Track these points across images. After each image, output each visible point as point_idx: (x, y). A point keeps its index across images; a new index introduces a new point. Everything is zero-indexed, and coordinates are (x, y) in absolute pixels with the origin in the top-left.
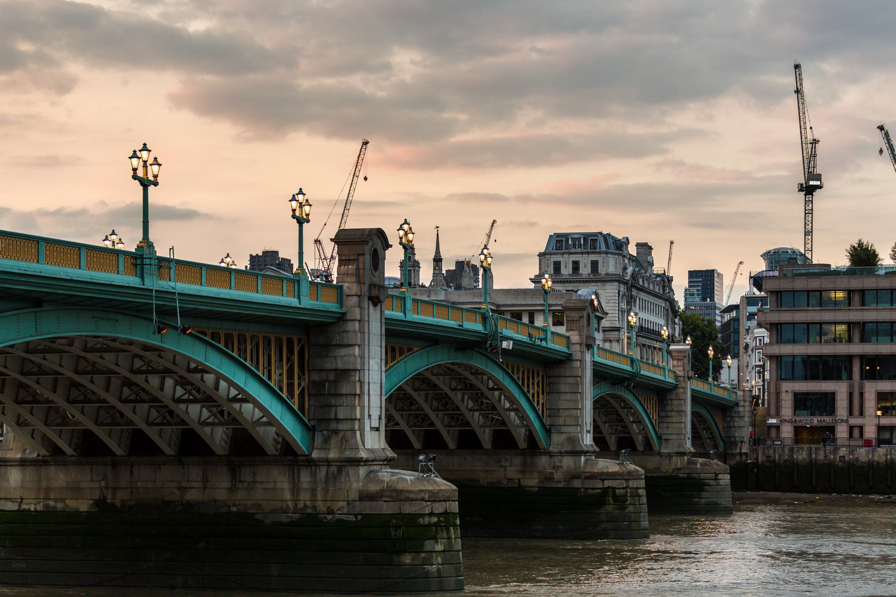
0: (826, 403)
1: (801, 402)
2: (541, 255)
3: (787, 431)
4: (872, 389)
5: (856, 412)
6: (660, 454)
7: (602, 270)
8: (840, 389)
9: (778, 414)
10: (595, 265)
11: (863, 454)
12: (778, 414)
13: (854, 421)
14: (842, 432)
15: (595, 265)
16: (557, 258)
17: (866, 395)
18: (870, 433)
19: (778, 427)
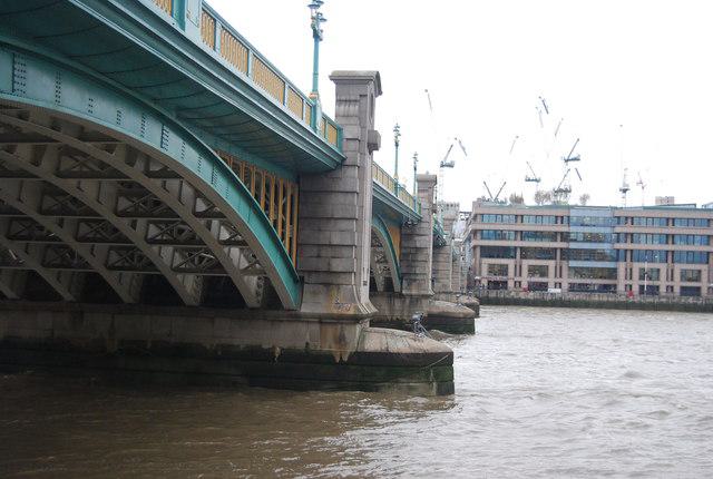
0: (504, 270)
3: (485, 282)
4: (526, 263)
8: (510, 263)
11: (522, 295)
12: (480, 274)
13: (517, 279)
14: (511, 284)
18: (525, 285)
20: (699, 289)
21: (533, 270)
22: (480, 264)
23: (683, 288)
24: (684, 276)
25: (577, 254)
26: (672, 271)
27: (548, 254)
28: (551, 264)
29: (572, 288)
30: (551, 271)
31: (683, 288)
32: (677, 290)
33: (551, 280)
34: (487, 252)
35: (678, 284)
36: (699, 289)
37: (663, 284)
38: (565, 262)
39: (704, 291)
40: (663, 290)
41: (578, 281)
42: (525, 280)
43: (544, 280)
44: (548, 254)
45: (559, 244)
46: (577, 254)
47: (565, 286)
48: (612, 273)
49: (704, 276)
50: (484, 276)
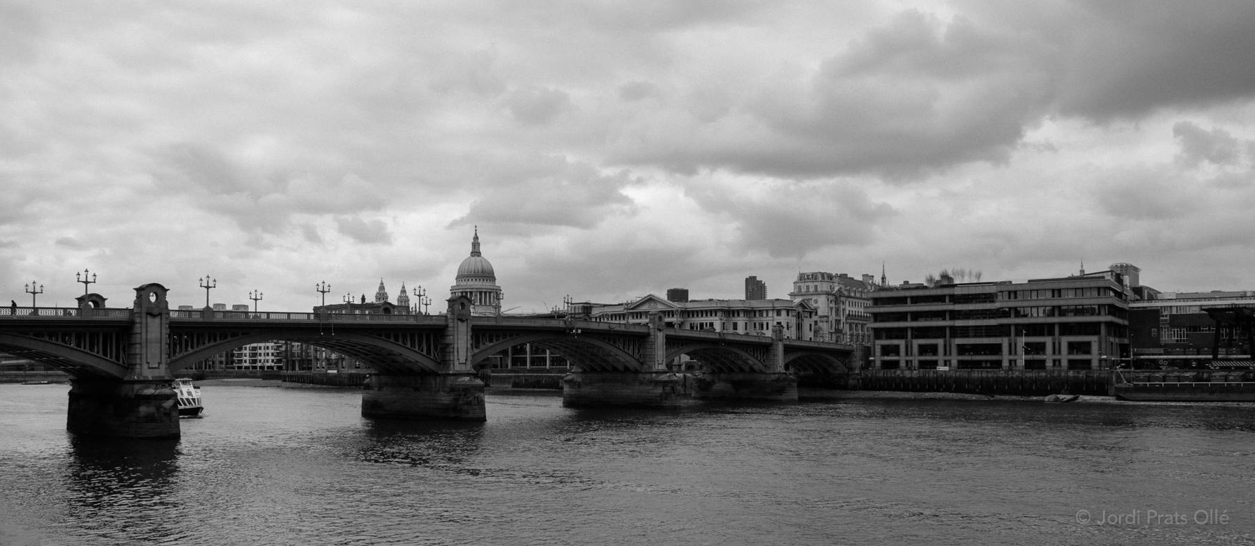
1: (886, 350)
2: (794, 283)
3: (878, 364)
5: (909, 354)
6: (765, 373)
7: (819, 289)
9: (874, 356)
10: (816, 287)
11: (907, 374)
12: (874, 356)
14: (903, 364)
15: (816, 287)
16: (800, 284)
17: (914, 346)
18: (916, 364)
19: (874, 361)
20: (1089, 362)
21: (923, 350)
22: (874, 345)
23: (1070, 361)
24: (1073, 347)
25: (964, 332)
26: (1060, 344)
27: (939, 332)
28: (940, 342)
29: (962, 364)
30: (941, 349)
31: (1070, 361)
32: (1065, 363)
33: (940, 357)
34: (878, 333)
35: (1065, 357)
36: (1089, 362)
37: (1048, 357)
38: (952, 340)
39: (1095, 364)
40: (1049, 364)
41: (966, 358)
42: (916, 359)
43: (934, 358)
44: (939, 332)
45: (947, 323)
46: (964, 332)
47: (954, 363)
48: (997, 349)
49: (1095, 348)
50: (877, 358)
